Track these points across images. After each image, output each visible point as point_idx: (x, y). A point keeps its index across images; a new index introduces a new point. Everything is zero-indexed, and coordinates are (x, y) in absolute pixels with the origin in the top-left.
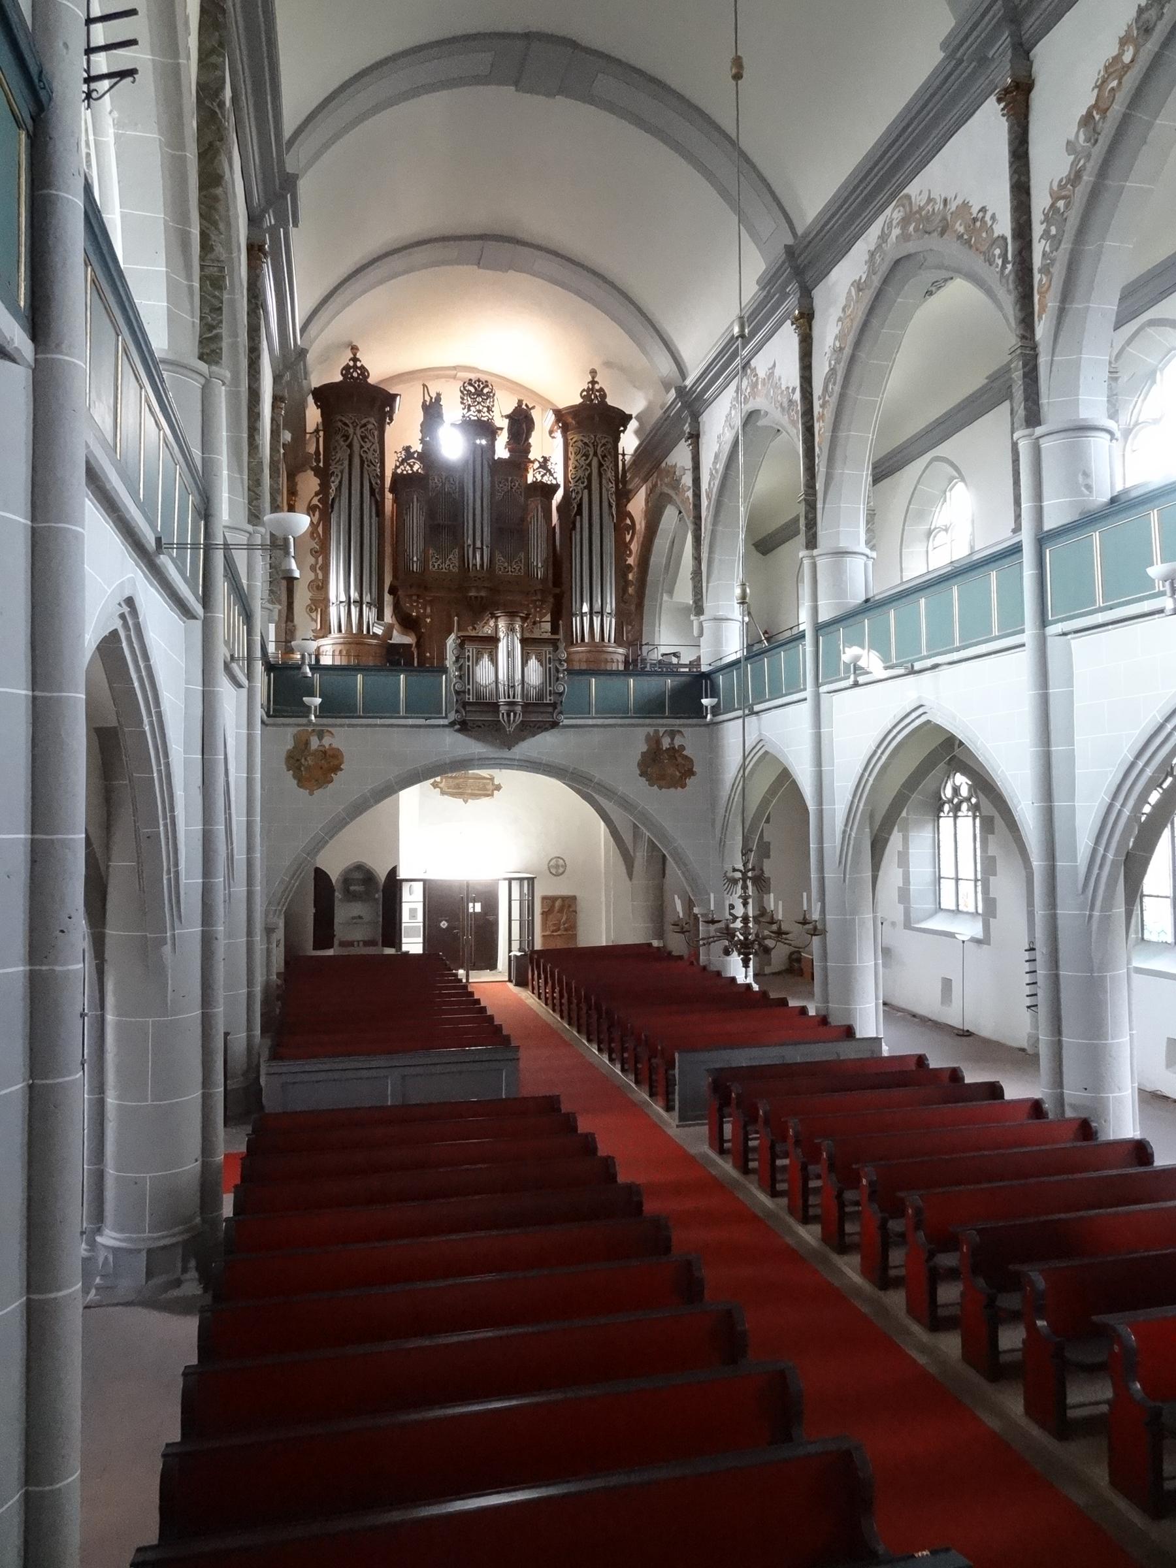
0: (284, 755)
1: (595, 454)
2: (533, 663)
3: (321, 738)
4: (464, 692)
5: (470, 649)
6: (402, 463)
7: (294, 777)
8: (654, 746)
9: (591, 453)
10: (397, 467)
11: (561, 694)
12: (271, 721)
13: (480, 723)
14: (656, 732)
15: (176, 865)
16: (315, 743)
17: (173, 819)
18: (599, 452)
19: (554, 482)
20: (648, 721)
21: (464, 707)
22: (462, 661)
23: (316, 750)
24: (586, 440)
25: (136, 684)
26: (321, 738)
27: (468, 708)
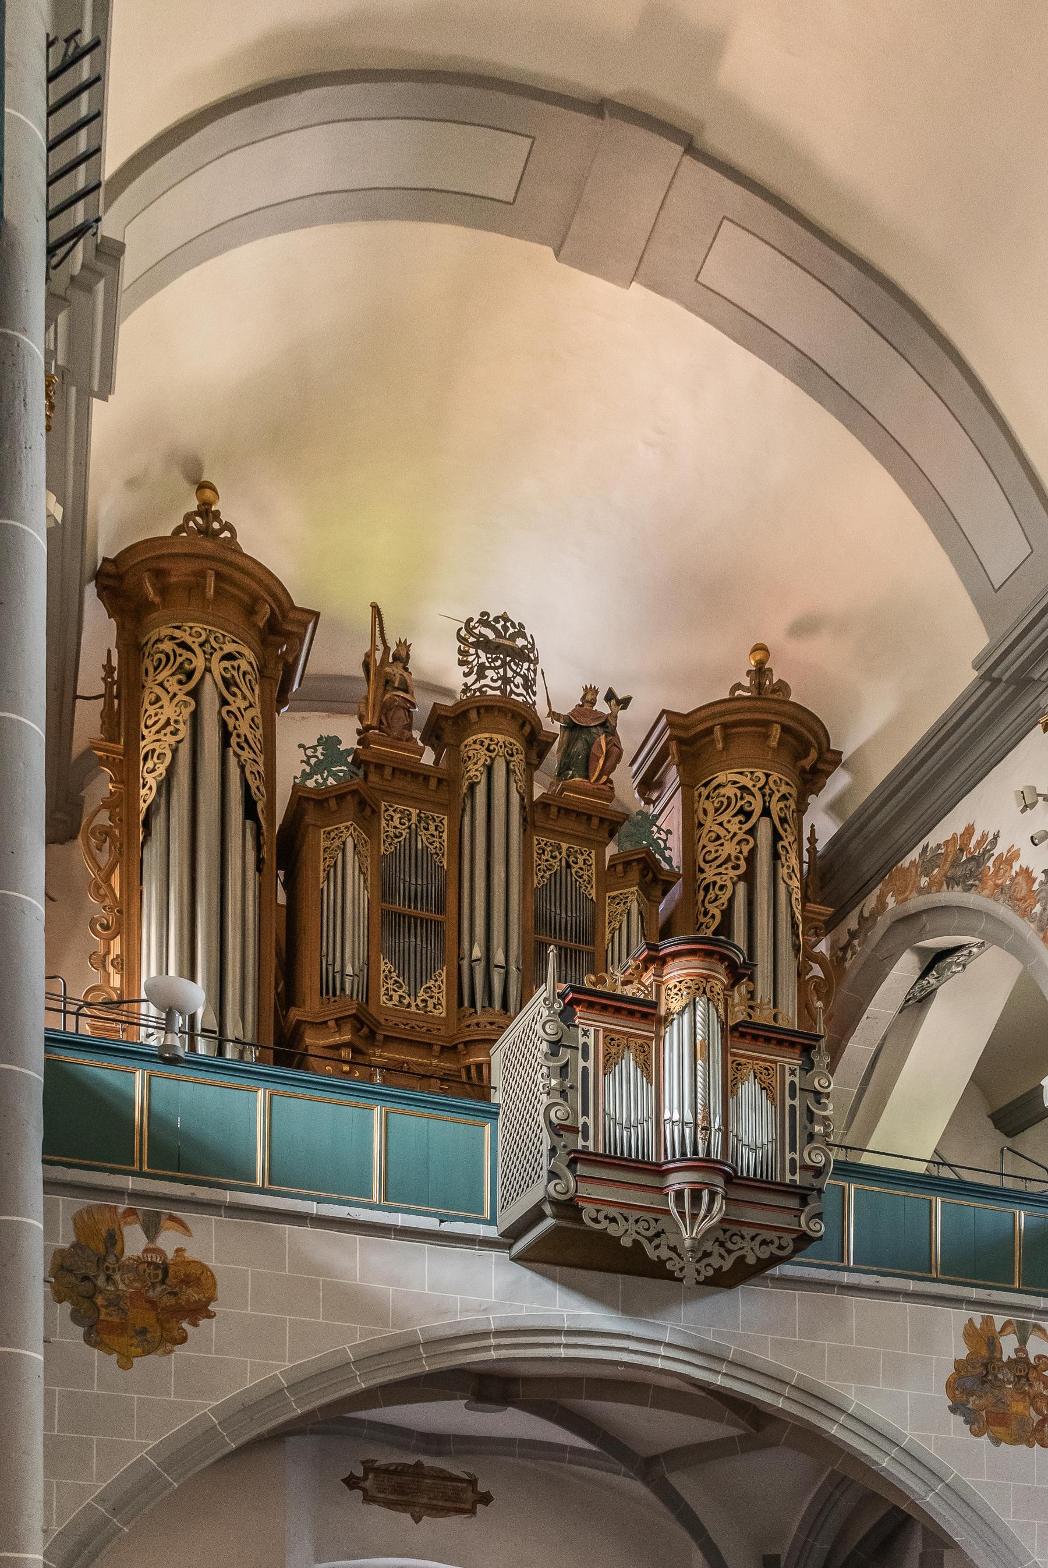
1: (766, 812)
2: (749, 1090)
4: (574, 1130)
5: (590, 1030)
6: (317, 769)
8: (984, 1352)
9: (757, 807)
10: (306, 776)
11: (818, 1172)
13: (613, 1212)
14: (988, 1322)
18: (775, 807)
19: (665, 866)
20: (975, 1293)
21: (572, 1164)
22: (566, 1055)
24: (746, 781)
27: (581, 1169)
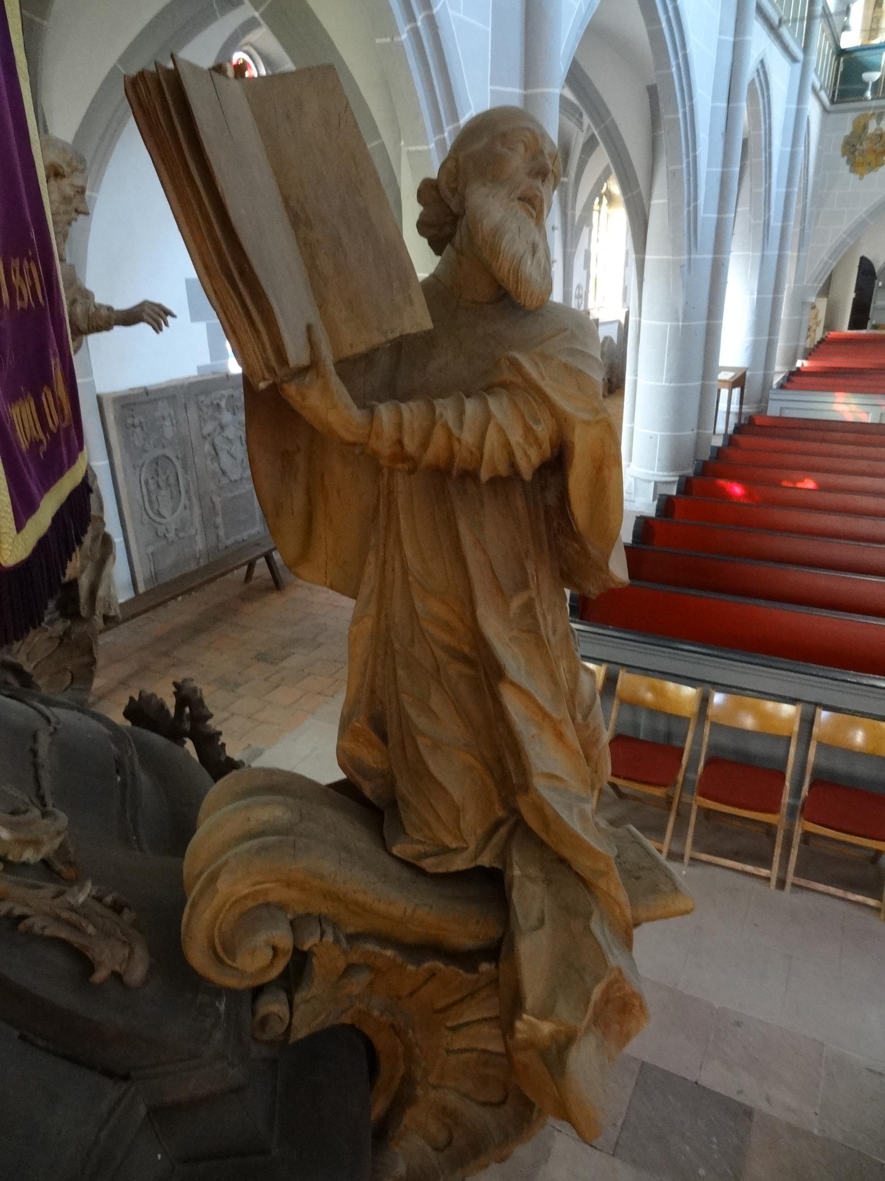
0: (841, 142)
3: (879, 122)
7: (848, 162)
12: (835, 107)
15: (696, 199)
16: (872, 127)
17: (695, 158)
23: (872, 134)
25: (664, 25)
26: (879, 122)
